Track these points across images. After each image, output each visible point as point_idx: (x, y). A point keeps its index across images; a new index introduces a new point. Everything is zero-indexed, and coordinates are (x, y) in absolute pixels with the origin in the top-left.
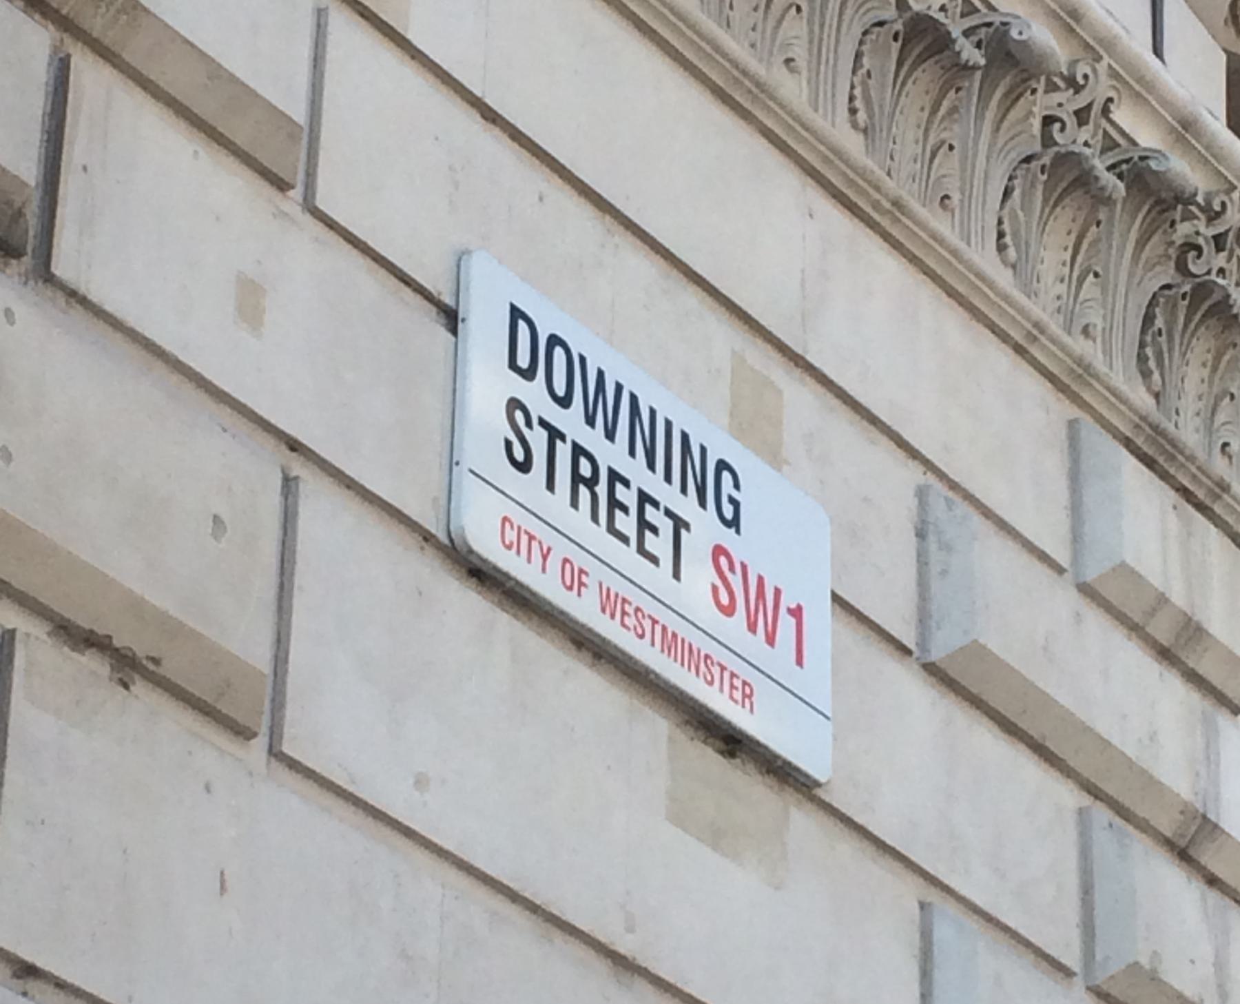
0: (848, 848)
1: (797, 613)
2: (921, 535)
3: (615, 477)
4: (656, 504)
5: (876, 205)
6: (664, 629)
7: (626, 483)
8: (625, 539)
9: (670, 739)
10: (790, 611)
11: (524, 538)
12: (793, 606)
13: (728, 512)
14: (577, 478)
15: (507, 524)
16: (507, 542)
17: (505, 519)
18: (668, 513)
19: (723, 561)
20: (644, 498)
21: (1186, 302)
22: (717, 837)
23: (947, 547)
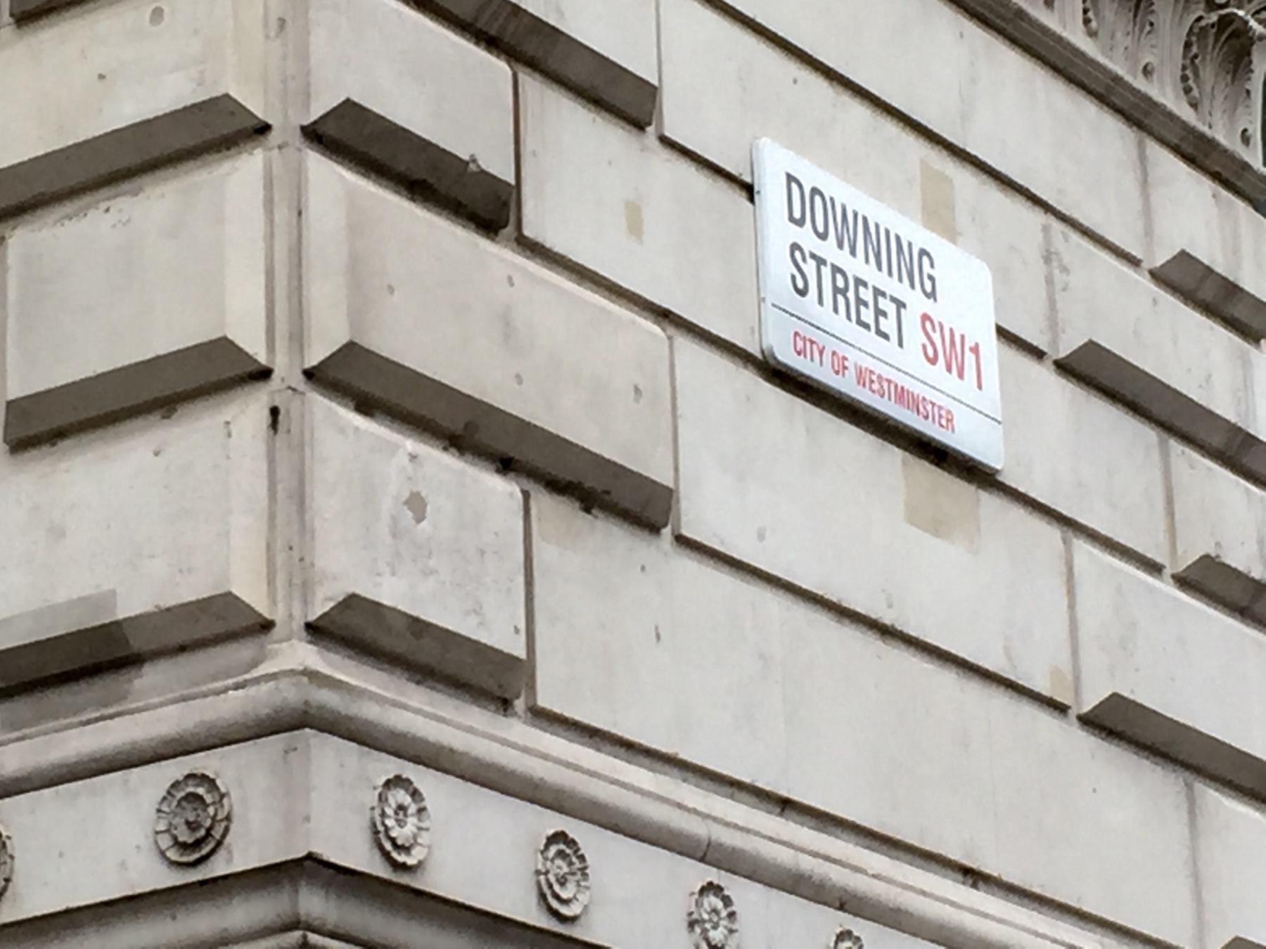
0: (1018, 513)
1: (975, 350)
2: (1047, 259)
3: (860, 282)
4: (884, 294)
5: (1004, 19)
6: (896, 386)
7: (865, 285)
8: (867, 326)
9: (904, 463)
10: (971, 349)
12: (973, 345)
14: (836, 290)
17: (796, 334)
18: (893, 300)
19: (928, 324)
20: (878, 293)
21: (1214, 30)
22: (937, 527)
23: (1065, 270)
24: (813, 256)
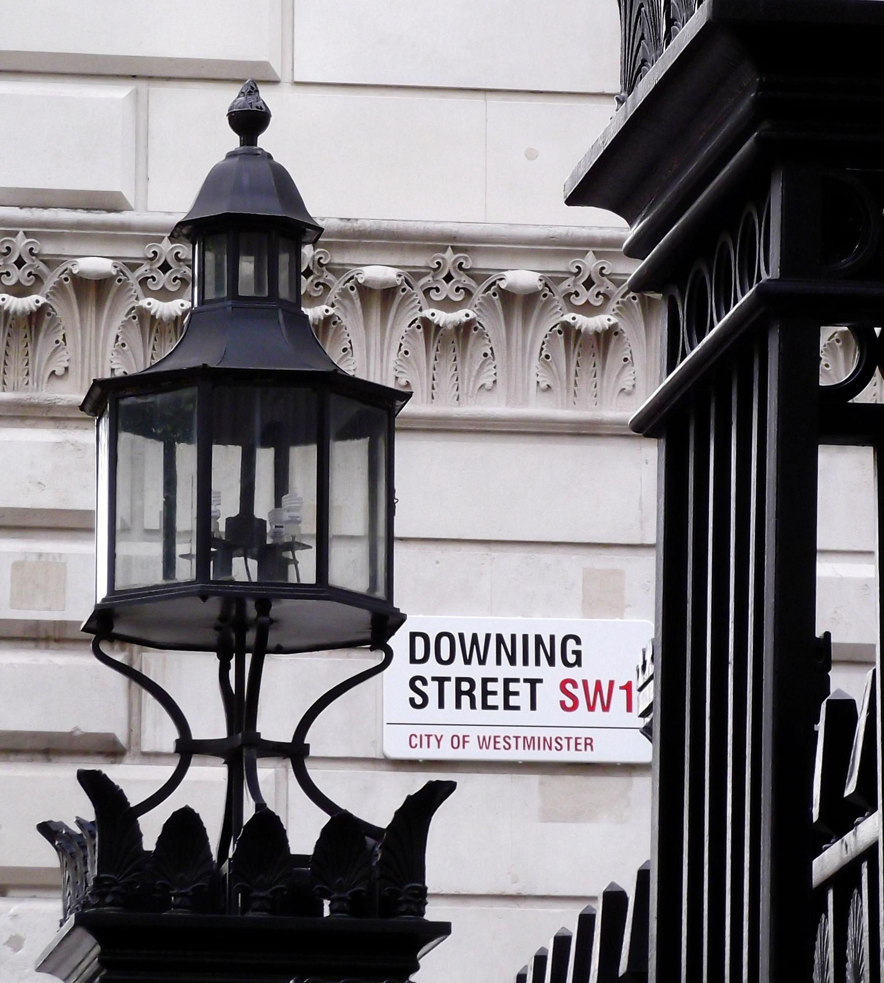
3: (485, 681)
4: (517, 680)
7: (495, 680)
8: (495, 708)
9: (541, 783)
10: (621, 688)
11: (425, 739)
12: (624, 683)
13: (571, 658)
14: (459, 693)
15: (413, 737)
16: (413, 745)
18: (526, 681)
20: (507, 681)
24: (434, 679)
